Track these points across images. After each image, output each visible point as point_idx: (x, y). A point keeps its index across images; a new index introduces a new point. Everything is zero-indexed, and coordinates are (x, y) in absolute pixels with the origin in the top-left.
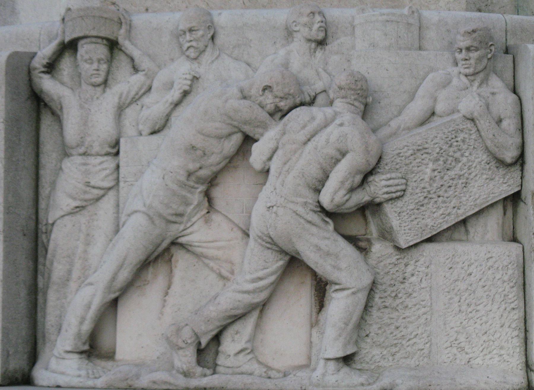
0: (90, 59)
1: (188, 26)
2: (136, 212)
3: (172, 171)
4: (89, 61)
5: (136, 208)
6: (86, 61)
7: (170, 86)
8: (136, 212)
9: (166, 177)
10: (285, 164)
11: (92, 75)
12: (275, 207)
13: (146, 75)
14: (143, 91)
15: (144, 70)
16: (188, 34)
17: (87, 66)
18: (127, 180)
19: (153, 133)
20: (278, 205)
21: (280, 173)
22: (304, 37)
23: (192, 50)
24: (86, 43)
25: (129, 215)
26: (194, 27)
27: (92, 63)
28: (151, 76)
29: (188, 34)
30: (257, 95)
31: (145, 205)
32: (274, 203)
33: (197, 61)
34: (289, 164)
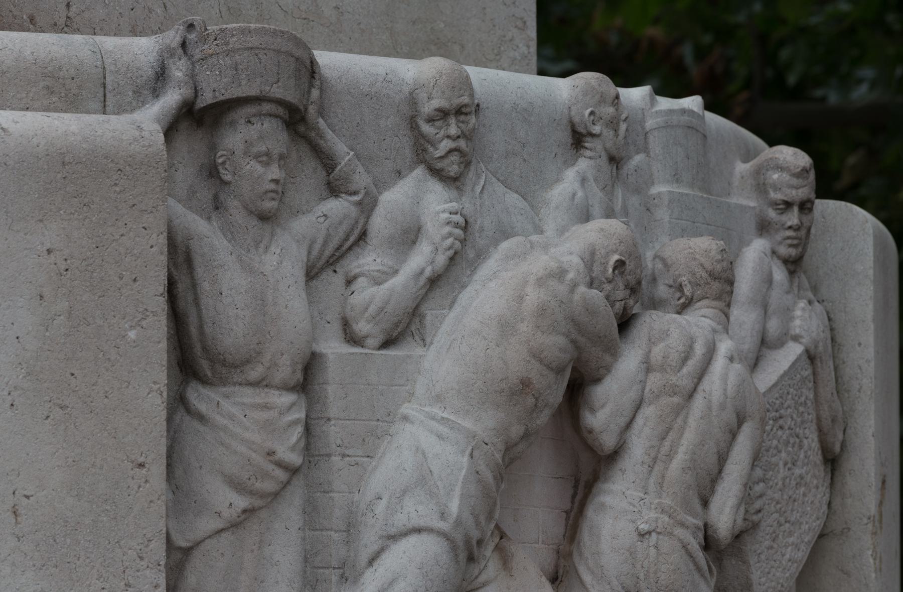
0: (267, 154)
1: (457, 102)
2: (418, 530)
3: (486, 441)
4: (265, 158)
5: (422, 523)
6: (257, 157)
7: (409, 236)
8: (418, 530)
9: (476, 453)
10: (663, 439)
11: (266, 192)
12: (653, 534)
13: (359, 203)
14: (352, 239)
15: (355, 193)
16: (452, 120)
17: (259, 168)
18: (347, 452)
19: (387, 343)
20: (659, 530)
21: (655, 460)
22: (606, 150)
23: (455, 157)
24: (260, 115)
25: (394, 538)
26: (466, 106)
27: (266, 164)
28: (367, 206)
29: (452, 120)
30: (603, 279)
31: (443, 516)
32: (654, 525)
33: (458, 184)
34: (669, 438)
